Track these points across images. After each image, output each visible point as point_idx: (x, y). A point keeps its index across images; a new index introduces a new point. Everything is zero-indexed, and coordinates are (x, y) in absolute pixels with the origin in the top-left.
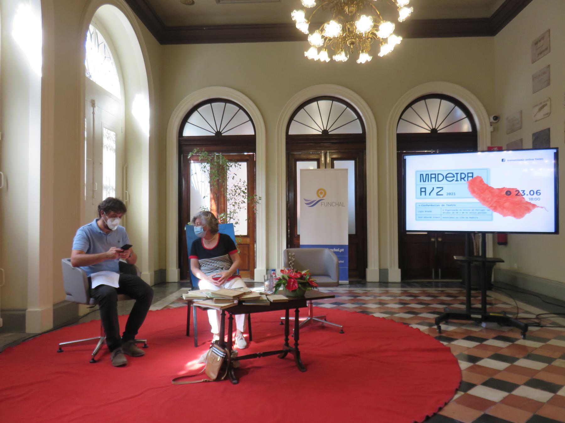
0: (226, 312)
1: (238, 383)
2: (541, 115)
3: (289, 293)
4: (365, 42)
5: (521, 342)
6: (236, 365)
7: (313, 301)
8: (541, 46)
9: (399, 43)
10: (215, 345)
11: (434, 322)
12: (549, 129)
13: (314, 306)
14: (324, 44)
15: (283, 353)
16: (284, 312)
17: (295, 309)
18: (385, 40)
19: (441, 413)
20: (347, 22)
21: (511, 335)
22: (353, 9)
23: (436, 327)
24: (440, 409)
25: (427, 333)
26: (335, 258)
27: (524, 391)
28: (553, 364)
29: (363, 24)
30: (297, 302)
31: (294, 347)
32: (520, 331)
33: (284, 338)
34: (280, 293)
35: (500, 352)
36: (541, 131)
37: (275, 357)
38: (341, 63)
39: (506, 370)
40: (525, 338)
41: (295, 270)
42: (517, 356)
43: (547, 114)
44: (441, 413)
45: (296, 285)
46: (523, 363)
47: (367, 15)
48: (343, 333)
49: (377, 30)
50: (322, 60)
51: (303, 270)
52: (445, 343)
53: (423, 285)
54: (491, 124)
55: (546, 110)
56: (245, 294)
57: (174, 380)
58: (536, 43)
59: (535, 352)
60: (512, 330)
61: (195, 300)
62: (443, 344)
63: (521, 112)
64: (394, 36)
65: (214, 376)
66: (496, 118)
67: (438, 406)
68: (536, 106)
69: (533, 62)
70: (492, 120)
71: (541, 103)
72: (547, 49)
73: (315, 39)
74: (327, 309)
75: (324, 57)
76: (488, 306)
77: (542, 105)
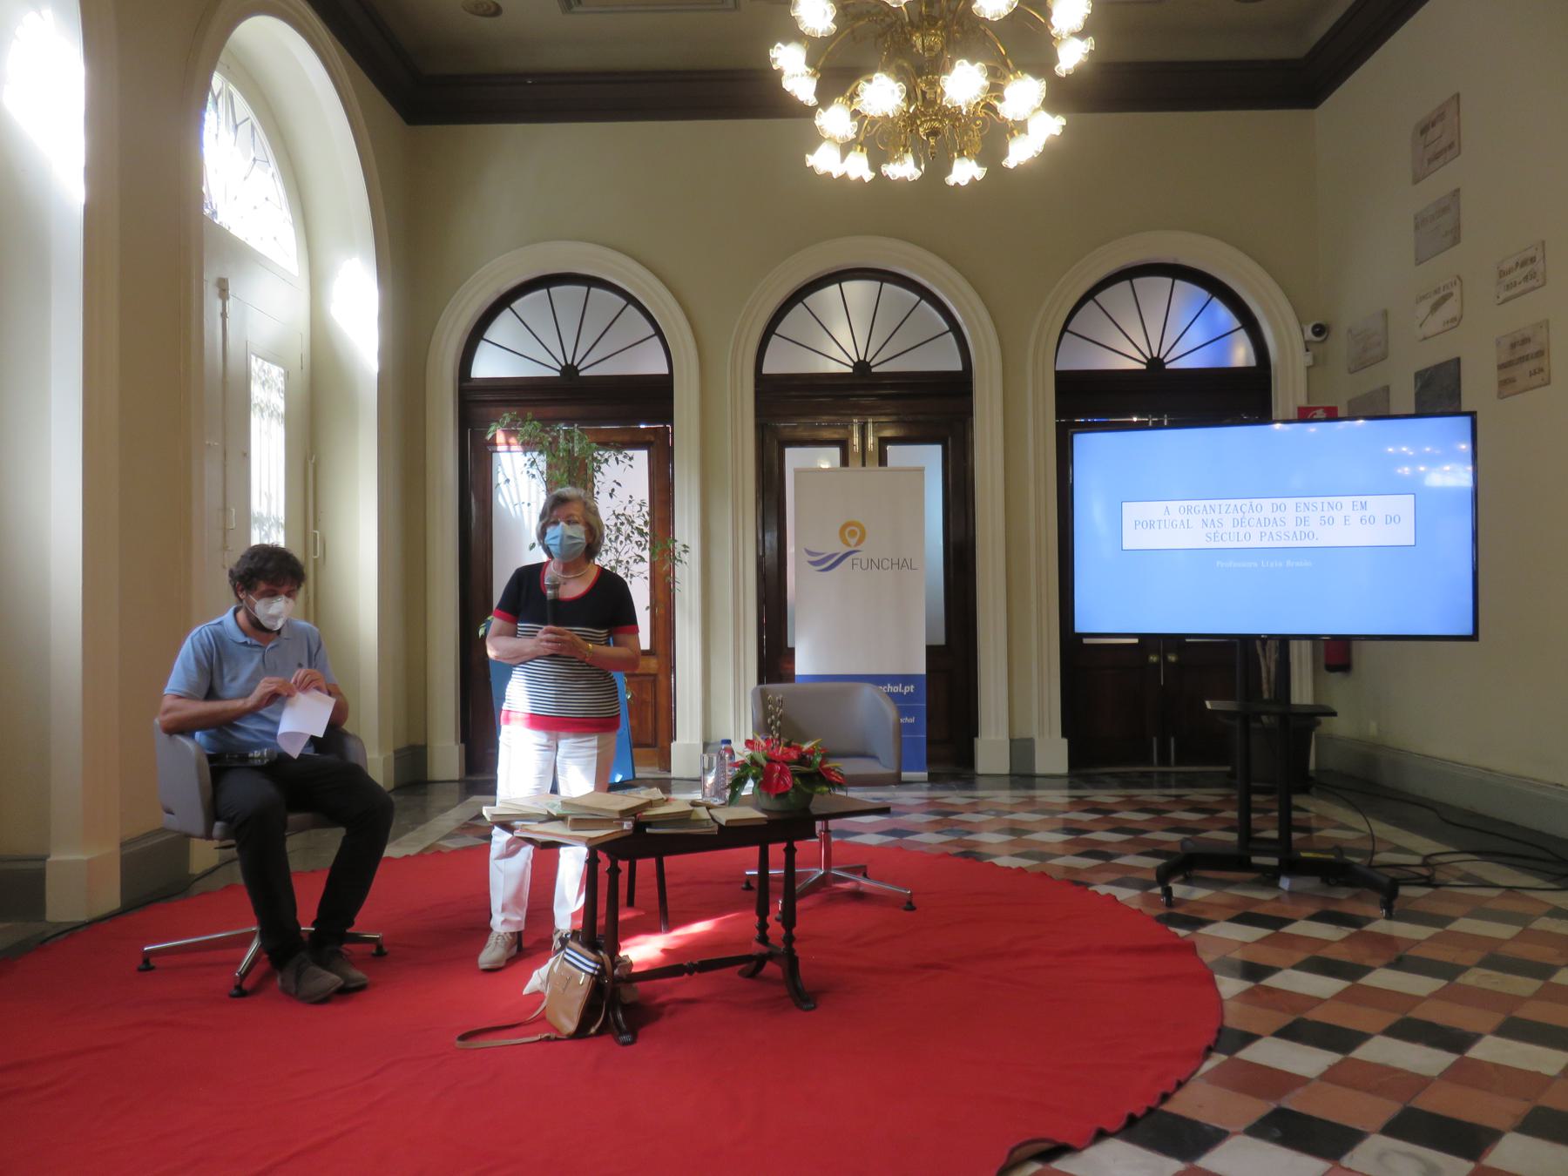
0: (602, 856)
3: (769, 802)
4: (966, 129)
5: (1381, 926)
6: (629, 994)
7: (834, 824)
8: (1437, 138)
10: (572, 944)
12: (1458, 360)
14: (857, 133)
15: (754, 963)
16: (753, 852)
17: (784, 845)
18: (1021, 127)
19: (1168, 1107)
20: (920, 71)
22: (935, 40)
23: (1158, 890)
24: (1166, 1097)
25: (1135, 907)
26: (890, 711)
27: (1381, 1051)
28: (1460, 980)
29: (963, 83)
30: (790, 823)
31: (783, 947)
32: (1378, 897)
34: (746, 801)
36: (1439, 367)
37: (731, 973)
38: (903, 182)
39: (1340, 996)
40: (1389, 917)
41: (784, 740)
42: (1368, 963)
43: (1454, 319)
44: (1168, 1107)
45: (788, 779)
46: (1382, 978)
47: (973, 61)
48: (913, 909)
49: (1001, 99)
50: (853, 176)
51: (806, 740)
52: (1182, 932)
53: (1126, 782)
54: (1308, 346)
56: (650, 804)
57: (463, 1038)
58: (1424, 131)
59: (1414, 952)
60: (1357, 897)
61: (517, 823)
63: (1385, 314)
64: (1044, 116)
65: (570, 1026)
66: (1320, 330)
67: (1159, 1091)
68: (1424, 297)
69: (1416, 181)
70: (1309, 334)
71: (1436, 292)
72: (1451, 146)
73: (835, 121)
74: (869, 846)
75: (858, 167)
76: (1296, 836)
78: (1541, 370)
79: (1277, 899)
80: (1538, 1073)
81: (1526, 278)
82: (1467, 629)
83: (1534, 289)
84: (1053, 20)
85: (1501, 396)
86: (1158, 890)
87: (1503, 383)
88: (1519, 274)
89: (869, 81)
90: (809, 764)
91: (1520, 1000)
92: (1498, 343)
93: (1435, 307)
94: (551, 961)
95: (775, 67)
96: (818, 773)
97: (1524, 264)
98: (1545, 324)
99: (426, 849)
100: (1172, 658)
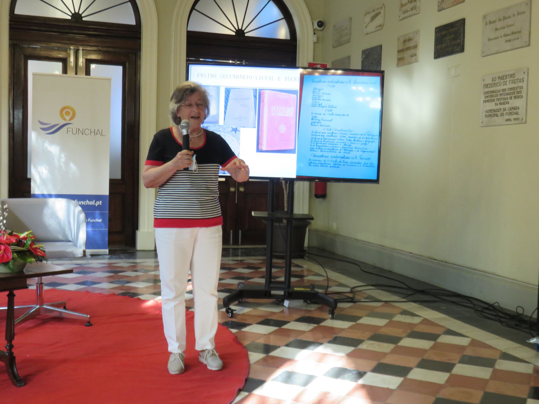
2: (372, 27)
5: (329, 323)
12: (381, 47)
13: (45, 288)
17: (7, 293)
21: (317, 315)
32: (328, 308)
40: (333, 318)
41: (9, 231)
43: (380, 26)
48: (91, 325)
52: (234, 331)
55: (379, 21)
60: (320, 309)
62: (231, 332)
63: (351, 19)
66: (321, 24)
68: (368, 13)
71: (374, 11)
74: (70, 292)
76: (293, 280)
77: (375, 13)
79: (282, 312)
80: (388, 389)
81: (412, 9)
82: (375, 178)
85: (398, 65)
86: (224, 310)
90: (23, 245)
91: (384, 355)
96: (29, 251)
98: (417, 32)
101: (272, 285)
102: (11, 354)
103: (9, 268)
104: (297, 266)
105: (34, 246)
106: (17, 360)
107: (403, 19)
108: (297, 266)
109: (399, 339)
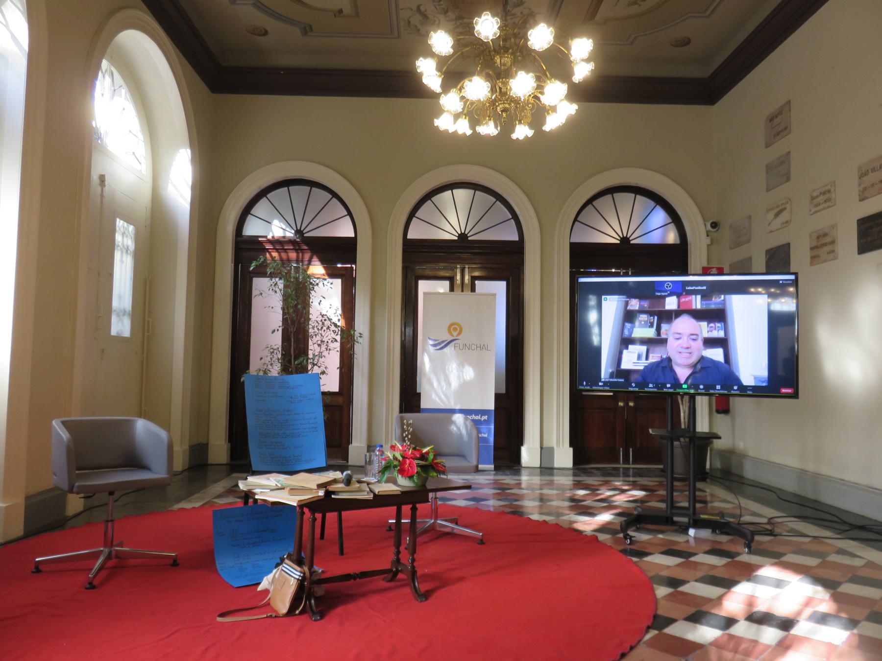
0: (306, 510)
1: (321, 619)
6: (320, 590)
8: (778, 124)
9: (573, 112)
10: (286, 561)
11: (619, 528)
12: (788, 245)
14: (463, 109)
18: (554, 109)
20: (498, 79)
22: (507, 60)
23: (621, 535)
29: (522, 84)
32: (743, 541)
33: (393, 550)
35: (716, 573)
36: (778, 248)
38: (487, 138)
40: (750, 552)
42: (737, 579)
43: (787, 222)
47: (528, 72)
49: (542, 93)
50: (460, 132)
51: (425, 447)
52: (635, 559)
53: (606, 473)
55: (784, 216)
57: (222, 615)
58: (771, 119)
60: (731, 541)
61: (257, 491)
63: (750, 217)
64: (566, 103)
66: (715, 225)
67: (620, 652)
68: (771, 209)
69: (767, 146)
72: (786, 128)
73: (451, 102)
74: (460, 507)
75: (463, 127)
76: (698, 505)
77: (778, 209)
78: (833, 251)
81: (825, 201)
83: (829, 207)
84: (572, 52)
85: (812, 264)
86: (621, 535)
87: (813, 258)
88: (821, 199)
89: (470, 81)
92: (810, 236)
93: (777, 215)
94: (275, 571)
95: (419, 71)
97: (824, 193)
98: (834, 226)
99: (205, 504)
100: (631, 404)
101: (674, 511)
102: (413, 567)
103: (414, 481)
104: (700, 490)
105: (438, 461)
106: (418, 574)
107: (815, 212)
108: (700, 490)
109: (839, 584)
